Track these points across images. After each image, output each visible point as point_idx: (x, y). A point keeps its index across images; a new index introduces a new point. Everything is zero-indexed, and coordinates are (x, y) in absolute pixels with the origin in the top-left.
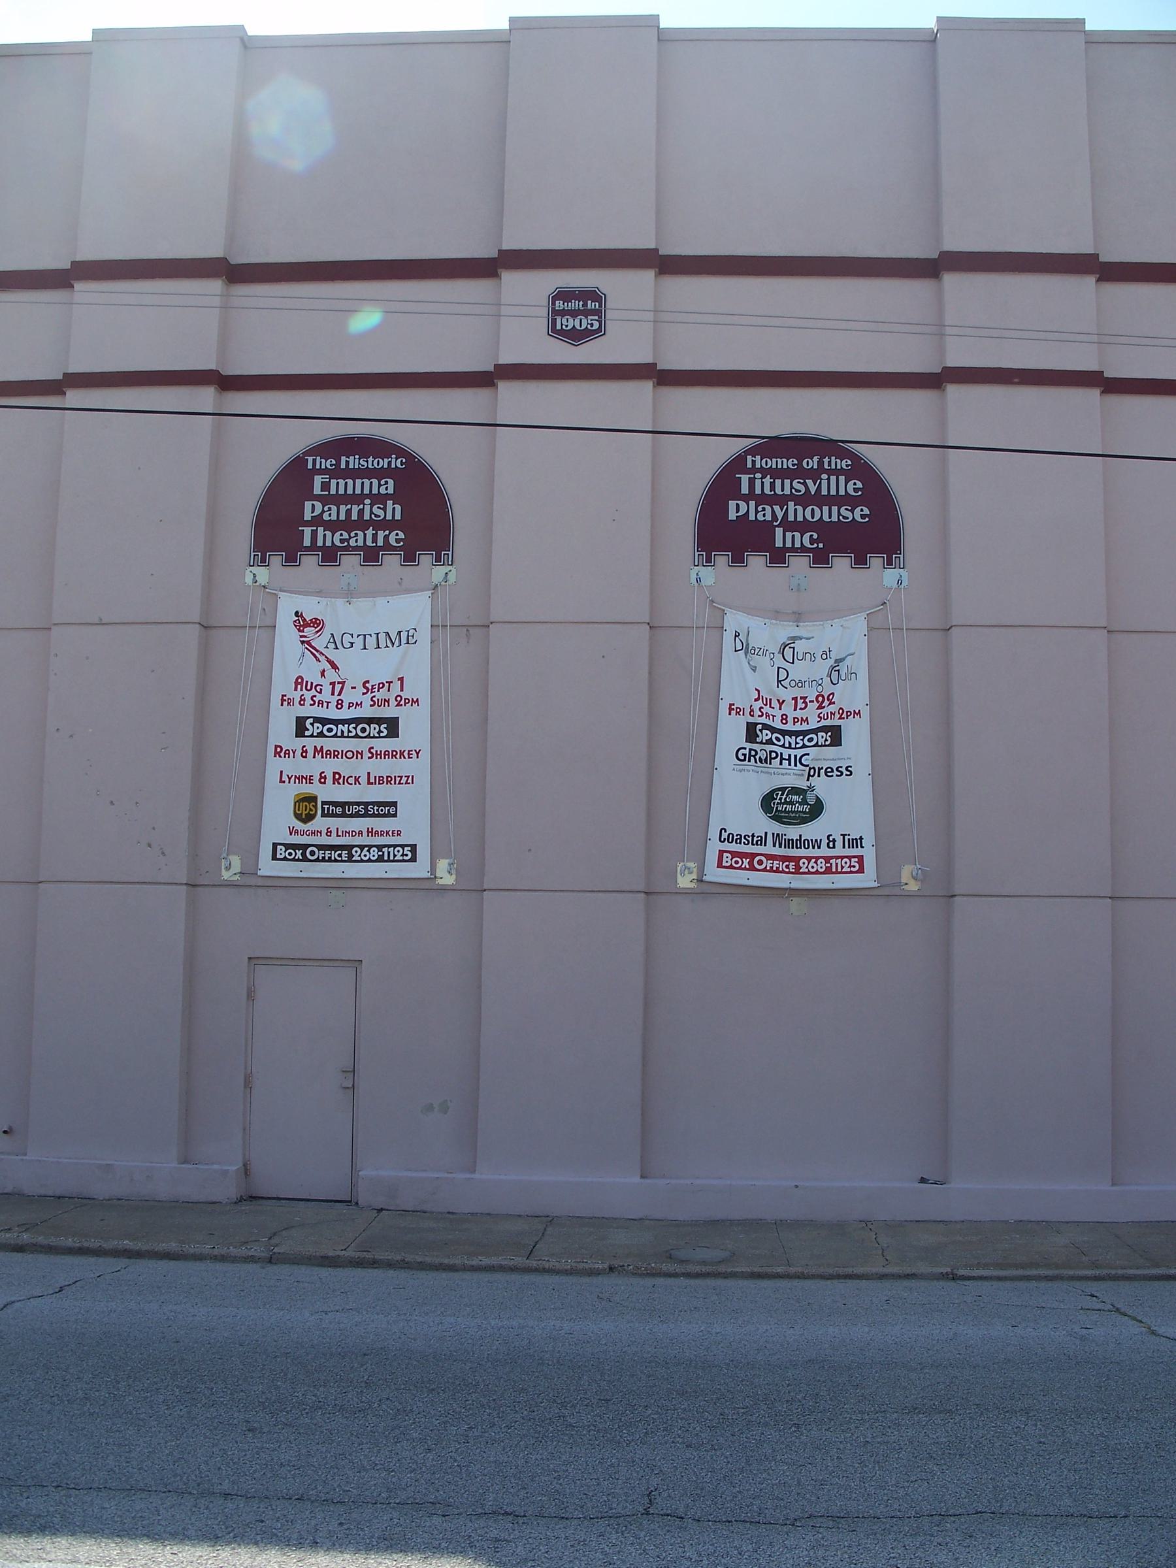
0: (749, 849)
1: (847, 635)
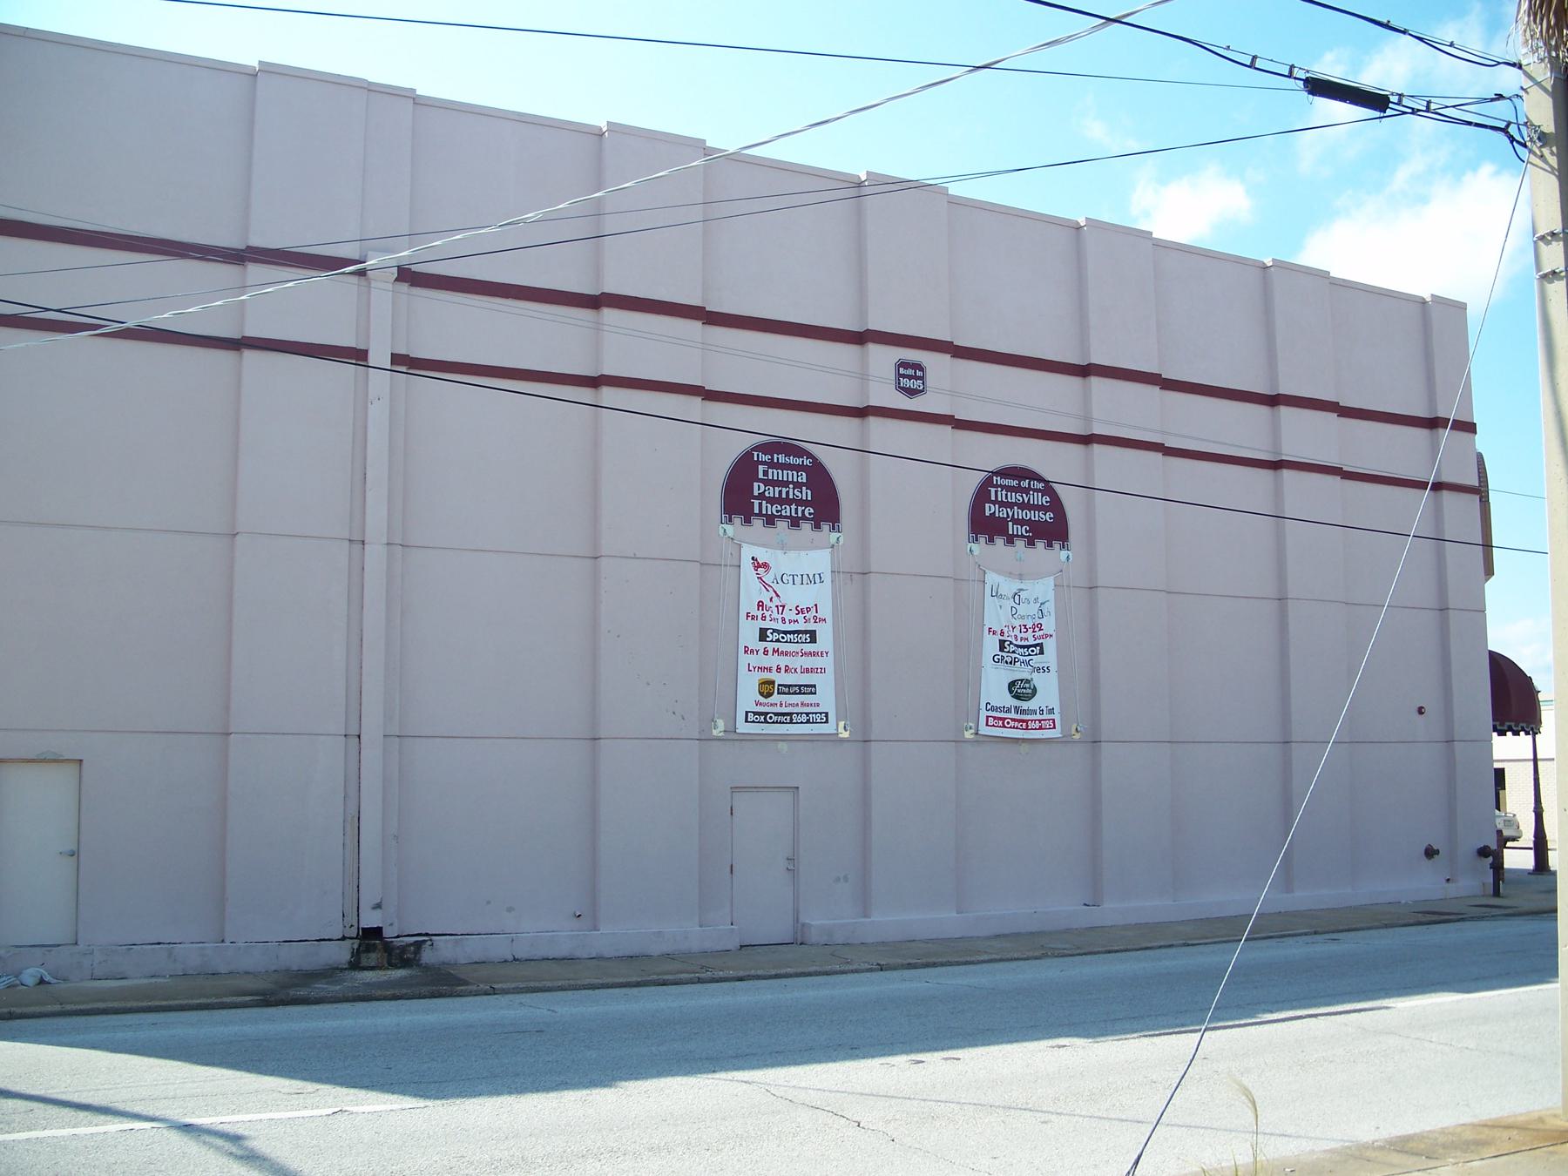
0: (1002, 715)
1: (1043, 589)
